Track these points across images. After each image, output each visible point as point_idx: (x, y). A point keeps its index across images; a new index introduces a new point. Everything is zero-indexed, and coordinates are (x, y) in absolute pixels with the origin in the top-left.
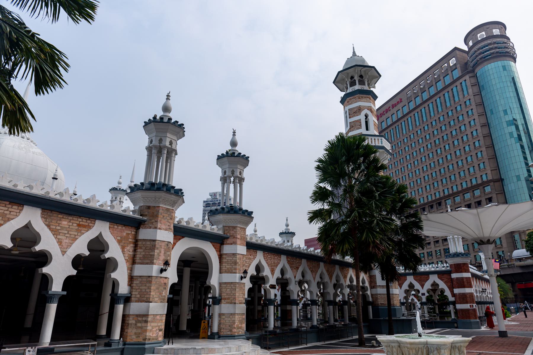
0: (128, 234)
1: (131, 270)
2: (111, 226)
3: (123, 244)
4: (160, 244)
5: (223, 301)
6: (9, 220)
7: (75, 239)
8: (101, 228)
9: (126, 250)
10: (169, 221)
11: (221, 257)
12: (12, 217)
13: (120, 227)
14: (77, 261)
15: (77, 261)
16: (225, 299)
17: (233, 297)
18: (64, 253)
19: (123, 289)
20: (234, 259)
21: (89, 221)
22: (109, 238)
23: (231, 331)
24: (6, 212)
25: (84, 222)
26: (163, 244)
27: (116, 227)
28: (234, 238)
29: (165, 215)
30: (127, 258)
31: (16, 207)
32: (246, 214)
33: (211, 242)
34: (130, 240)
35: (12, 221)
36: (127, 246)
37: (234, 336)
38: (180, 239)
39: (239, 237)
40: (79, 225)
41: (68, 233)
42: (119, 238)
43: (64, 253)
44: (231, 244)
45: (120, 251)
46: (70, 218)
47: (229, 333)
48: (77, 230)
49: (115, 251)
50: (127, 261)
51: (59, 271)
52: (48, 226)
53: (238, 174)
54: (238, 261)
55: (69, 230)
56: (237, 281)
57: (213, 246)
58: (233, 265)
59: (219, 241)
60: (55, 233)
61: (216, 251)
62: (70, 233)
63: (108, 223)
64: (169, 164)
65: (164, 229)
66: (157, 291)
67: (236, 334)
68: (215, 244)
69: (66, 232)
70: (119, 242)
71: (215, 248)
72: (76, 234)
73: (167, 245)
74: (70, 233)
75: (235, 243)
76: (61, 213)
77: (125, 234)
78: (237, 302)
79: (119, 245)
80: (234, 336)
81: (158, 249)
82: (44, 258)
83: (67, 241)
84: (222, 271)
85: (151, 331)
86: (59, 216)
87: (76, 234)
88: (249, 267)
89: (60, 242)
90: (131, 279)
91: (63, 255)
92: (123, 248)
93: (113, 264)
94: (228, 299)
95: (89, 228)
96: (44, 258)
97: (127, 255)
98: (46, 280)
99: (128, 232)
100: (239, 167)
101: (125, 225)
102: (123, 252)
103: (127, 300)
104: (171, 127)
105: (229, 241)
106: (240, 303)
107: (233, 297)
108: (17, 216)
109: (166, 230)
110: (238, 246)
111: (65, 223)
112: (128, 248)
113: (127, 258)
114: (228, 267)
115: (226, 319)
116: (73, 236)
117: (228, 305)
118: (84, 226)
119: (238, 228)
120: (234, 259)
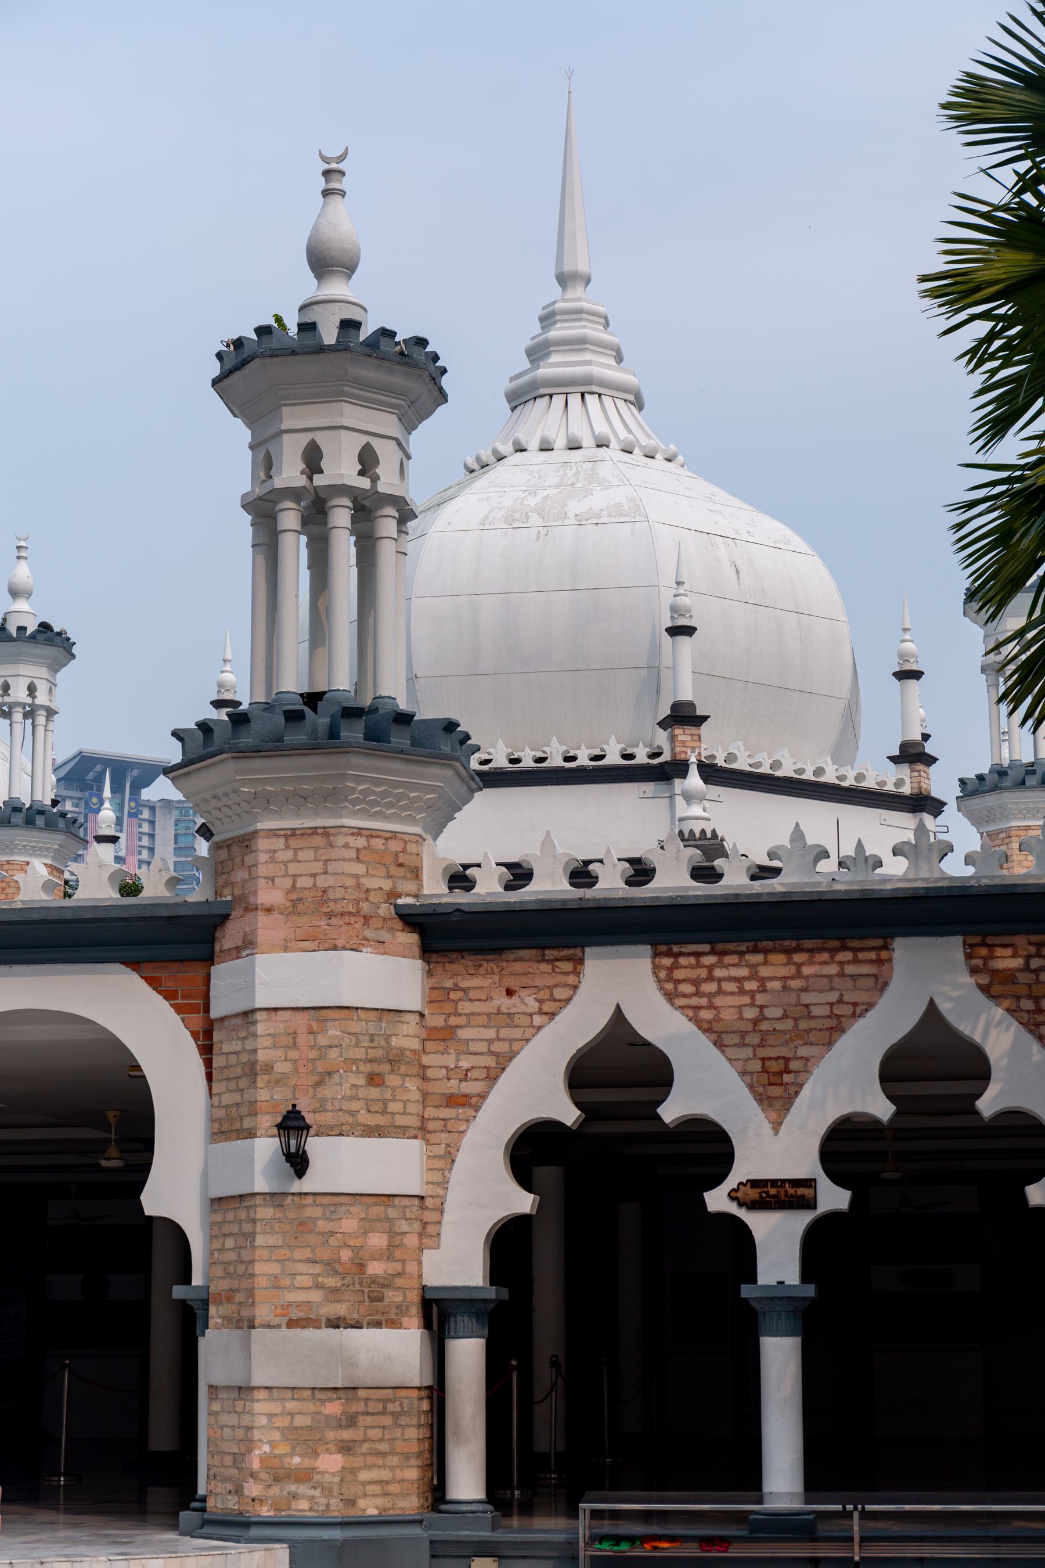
5: (212, 1310)
20: (249, 1045)
23: (238, 1491)
28: (247, 909)
32: (353, 732)
33: (134, 964)
37: (247, 1525)
39: (267, 895)
44: (237, 952)
47: (232, 1503)
54: (262, 1056)
56: (261, 1185)
57: (153, 982)
58: (243, 1083)
59: (175, 945)
61: (179, 1009)
67: (265, 1512)
68: (169, 975)
71: (169, 996)
75: (247, 945)
78: (263, 1312)
80: (247, 1525)
88: (492, 1077)
105: (229, 937)
106: (291, 1324)
107: (245, 1284)
110: (261, 960)
114: (228, 1099)
115: (224, 1419)
117: (225, 1331)
119: (262, 844)
120: (249, 1045)
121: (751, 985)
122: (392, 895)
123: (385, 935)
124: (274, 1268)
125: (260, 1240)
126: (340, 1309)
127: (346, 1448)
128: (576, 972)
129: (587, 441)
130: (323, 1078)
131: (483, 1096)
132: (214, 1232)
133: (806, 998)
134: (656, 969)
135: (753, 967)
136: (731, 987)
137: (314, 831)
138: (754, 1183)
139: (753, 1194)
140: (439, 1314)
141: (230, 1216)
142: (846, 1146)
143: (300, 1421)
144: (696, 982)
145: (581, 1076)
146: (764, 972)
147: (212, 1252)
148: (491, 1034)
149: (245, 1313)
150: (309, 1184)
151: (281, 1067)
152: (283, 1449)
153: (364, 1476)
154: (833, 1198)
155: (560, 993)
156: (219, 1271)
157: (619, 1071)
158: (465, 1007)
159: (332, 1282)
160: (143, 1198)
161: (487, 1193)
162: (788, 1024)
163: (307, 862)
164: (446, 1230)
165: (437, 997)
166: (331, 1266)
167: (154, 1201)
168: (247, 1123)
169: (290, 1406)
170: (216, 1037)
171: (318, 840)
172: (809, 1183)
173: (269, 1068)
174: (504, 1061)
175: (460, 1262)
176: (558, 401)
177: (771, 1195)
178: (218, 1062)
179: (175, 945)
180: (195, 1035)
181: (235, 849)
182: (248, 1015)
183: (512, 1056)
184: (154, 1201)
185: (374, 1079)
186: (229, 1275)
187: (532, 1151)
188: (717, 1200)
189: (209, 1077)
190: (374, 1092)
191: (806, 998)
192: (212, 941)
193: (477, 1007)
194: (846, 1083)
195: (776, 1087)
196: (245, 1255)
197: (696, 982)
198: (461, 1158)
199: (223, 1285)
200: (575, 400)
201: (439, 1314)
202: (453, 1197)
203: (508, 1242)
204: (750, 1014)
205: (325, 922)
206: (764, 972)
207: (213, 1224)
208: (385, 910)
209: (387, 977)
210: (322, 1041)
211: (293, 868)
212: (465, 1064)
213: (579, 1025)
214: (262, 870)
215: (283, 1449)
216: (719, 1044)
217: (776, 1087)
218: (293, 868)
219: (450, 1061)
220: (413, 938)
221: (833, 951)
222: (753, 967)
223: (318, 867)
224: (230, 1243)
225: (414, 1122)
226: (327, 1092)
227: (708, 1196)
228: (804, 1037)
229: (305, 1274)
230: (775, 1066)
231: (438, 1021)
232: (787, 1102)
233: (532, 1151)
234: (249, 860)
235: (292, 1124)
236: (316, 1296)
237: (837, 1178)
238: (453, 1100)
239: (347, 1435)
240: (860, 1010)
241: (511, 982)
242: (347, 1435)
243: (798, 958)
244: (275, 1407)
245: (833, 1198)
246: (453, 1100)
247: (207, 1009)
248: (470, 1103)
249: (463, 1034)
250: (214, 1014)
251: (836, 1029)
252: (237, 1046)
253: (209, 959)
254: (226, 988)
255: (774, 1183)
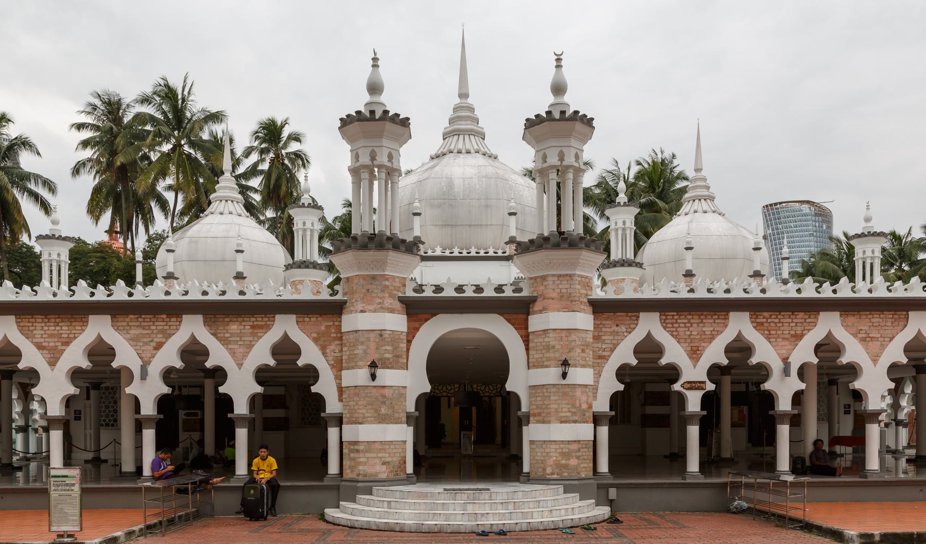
0: (328, 327)
1: (338, 378)
2: (300, 320)
3: (322, 343)
4: (367, 336)
5: (531, 418)
6: (170, 335)
7: (250, 347)
8: (285, 326)
9: (328, 351)
10: (380, 295)
11: (526, 339)
12: (173, 332)
13: (313, 319)
14: (262, 375)
15: (262, 375)
16: (534, 415)
17: (546, 411)
18: (240, 365)
19: (333, 406)
20: (546, 340)
21: (266, 319)
22: (299, 337)
24: (165, 327)
25: (260, 321)
26: (372, 335)
27: (307, 319)
29: (369, 287)
30: (332, 362)
31: (174, 319)
34: (333, 335)
35: (173, 337)
36: (330, 345)
38: (426, 320)
40: (253, 327)
41: (241, 340)
42: (315, 335)
43: (240, 365)
44: (540, 312)
45: (320, 353)
46: (240, 319)
48: (253, 334)
49: (310, 354)
50: (332, 367)
51: (241, 388)
52: (214, 335)
53: (573, 159)
55: (241, 335)
57: (509, 321)
58: (544, 351)
60: (224, 341)
61: (516, 329)
62: (243, 339)
63: (294, 316)
64: (389, 193)
65: (370, 311)
66: (370, 407)
69: (238, 339)
70: (315, 340)
71: (513, 324)
72: (251, 339)
73: (381, 335)
74: (243, 339)
76: (227, 315)
77: (323, 328)
79: (317, 345)
81: (363, 343)
82: (219, 374)
83: (241, 350)
84: (531, 365)
85: (365, 463)
86: (227, 319)
87: (251, 339)
88: (612, 351)
89: (233, 353)
90: (341, 390)
91: (240, 369)
92: (323, 349)
93: (312, 374)
94: (539, 414)
95: (268, 328)
96: (219, 374)
97: (330, 358)
98: (226, 402)
99: (323, 324)
100: (573, 142)
101: (321, 315)
102: (324, 354)
103: (339, 421)
104: (388, 126)
105: (537, 306)
108: (178, 330)
109: (375, 311)
111: (234, 327)
112: (332, 347)
113: (332, 362)
114: (536, 356)
116: (248, 343)
118: (261, 327)
120: (546, 340)
121: (688, 325)
122: (587, 295)
123: (585, 308)
124: (556, 406)
125: (552, 398)
126: (576, 418)
127: (578, 458)
128: (637, 320)
129: (472, 151)
130: (571, 350)
131: (609, 356)
132: (531, 395)
133: (704, 329)
134: (661, 319)
135: (689, 319)
136: (682, 325)
137: (567, 275)
138: (689, 382)
139: (689, 386)
140: (597, 420)
141: (539, 391)
142: (715, 371)
143: (564, 450)
144: (672, 324)
145: (637, 351)
146: (692, 321)
147: (530, 402)
148: (612, 338)
149: (546, 419)
150: (568, 381)
151: (557, 347)
152: (560, 458)
153: (582, 466)
154: (710, 387)
155: (632, 326)
156: (534, 407)
157: (649, 349)
158: (604, 330)
159: (573, 410)
160: (506, 385)
161: (610, 385)
162: (698, 337)
163: (564, 285)
164: (599, 395)
165: (596, 326)
166: (573, 406)
167: (509, 387)
168: (546, 363)
169: (562, 446)
170: (531, 337)
171: (568, 278)
172: (704, 382)
173: (553, 347)
174: (615, 346)
175: (602, 405)
176: (461, 137)
177: (693, 385)
178: (531, 345)
179: (517, 309)
180: (522, 337)
181: (538, 280)
182: (545, 331)
183: (618, 344)
184: (509, 387)
185: (583, 351)
186: (537, 408)
187: (622, 373)
188: (677, 387)
189: (527, 349)
190: (584, 355)
191: (704, 329)
192: (529, 308)
193: (608, 330)
194: (715, 353)
195: (695, 354)
196: (546, 402)
197: (672, 324)
198: (603, 374)
199: (536, 411)
200: (467, 137)
201: (597, 420)
202: (600, 386)
203: (615, 398)
204: (688, 333)
205: (568, 303)
206: (692, 321)
207: (530, 394)
208: (586, 300)
209: (584, 320)
210: (570, 339)
211: (560, 286)
212: (604, 346)
213: (637, 336)
214: (551, 287)
215: (560, 458)
216: (679, 342)
217: (695, 354)
218: (560, 286)
219: (599, 345)
220: (590, 309)
221: (712, 316)
222: (689, 319)
223: (568, 286)
224: (539, 399)
225: (591, 363)
226: (572, 354)
227: (675, 385)
228: (702, 340)
229: (566, 408)
230: (695, 349)
231: (596, 334)
232: (698, 360)
233: (622, 373)
234: (545, 283)
235: (565, 363)
236: (569, 414)
237: (712, 381)
238: (600, 357)
239: (578, 454)
240: (719, 333)
241: (618, 323)
242: (578, 454)
243: (702, 317)
244: (557, 447)
245: (710, 387)
246: (600, 357)
247: (527, 328)
248: (605, 358)
249: (603, 338)
250: (530, 330)
251: (712, 338)
252: (541, 340)
253: (528, 314)
254: (536, 322)
255: (694, 382)
